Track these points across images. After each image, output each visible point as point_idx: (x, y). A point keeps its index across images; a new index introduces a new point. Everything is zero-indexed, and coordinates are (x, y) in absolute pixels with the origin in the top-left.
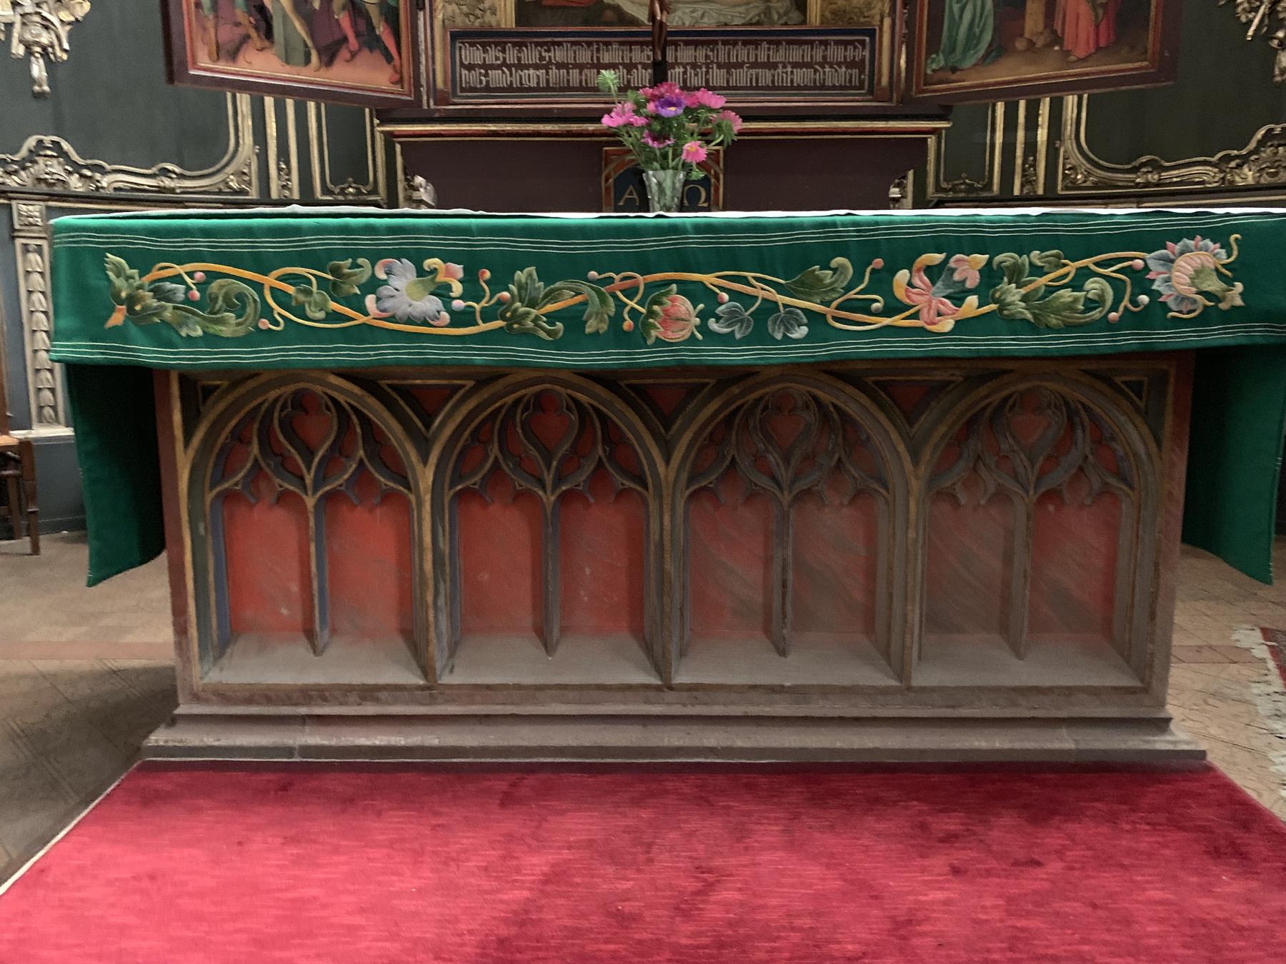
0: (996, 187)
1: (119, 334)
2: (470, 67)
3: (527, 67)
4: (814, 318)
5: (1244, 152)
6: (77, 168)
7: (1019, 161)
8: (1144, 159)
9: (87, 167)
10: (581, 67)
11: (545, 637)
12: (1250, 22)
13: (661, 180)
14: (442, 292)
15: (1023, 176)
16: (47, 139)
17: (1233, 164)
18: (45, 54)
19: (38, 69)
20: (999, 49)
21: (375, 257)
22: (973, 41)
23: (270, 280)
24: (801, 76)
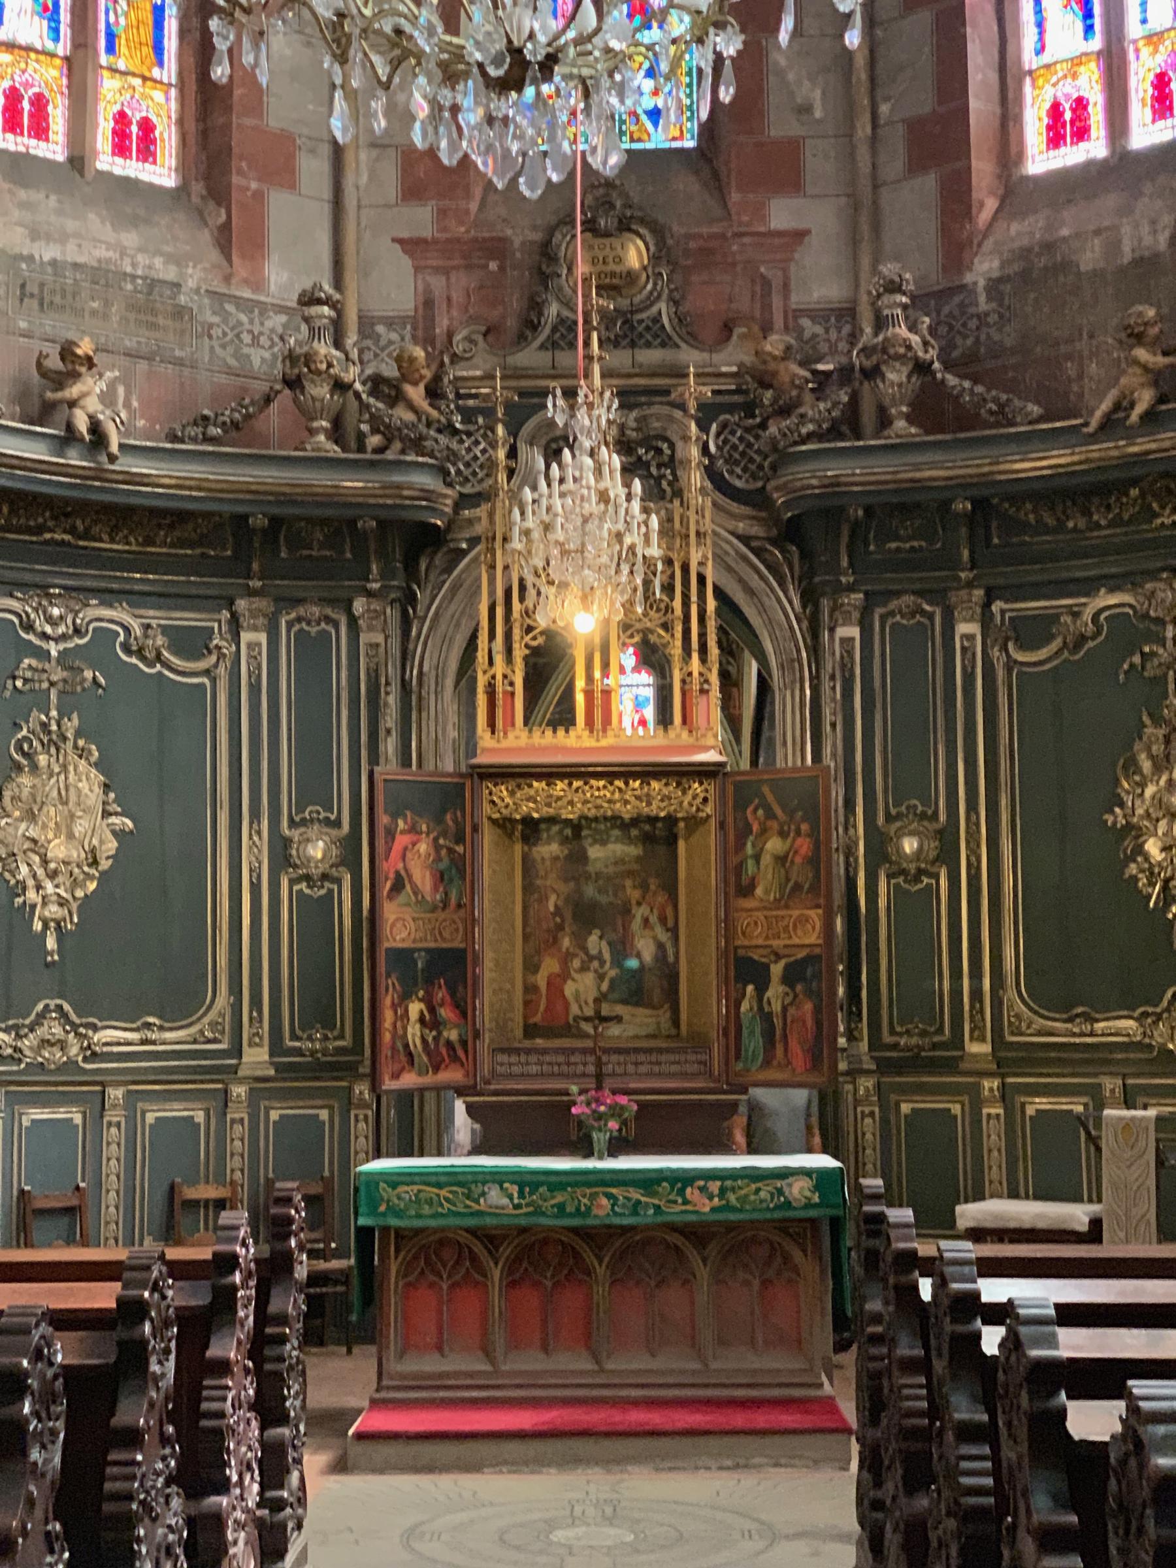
0: (947, 1031)
2: (502, 1064)
4: (657, 1208)
5: (1158, 1010)
6: (75, 1027)
7: (967, 1007)
8: (1080, 1010)
9: (81, 1025)
10: (559, 1065)
11: (545, 1348)
12: (1150, 896)
13: (600, 1139)
14: (511, 1197)
15: (972, 1021)
16: (52, 1003)
17: (1149, 1020)
18: (58, 927)
19: (51, 943)
20: (767, 1063)
21: (484, 1184)
24: (674, 1068)
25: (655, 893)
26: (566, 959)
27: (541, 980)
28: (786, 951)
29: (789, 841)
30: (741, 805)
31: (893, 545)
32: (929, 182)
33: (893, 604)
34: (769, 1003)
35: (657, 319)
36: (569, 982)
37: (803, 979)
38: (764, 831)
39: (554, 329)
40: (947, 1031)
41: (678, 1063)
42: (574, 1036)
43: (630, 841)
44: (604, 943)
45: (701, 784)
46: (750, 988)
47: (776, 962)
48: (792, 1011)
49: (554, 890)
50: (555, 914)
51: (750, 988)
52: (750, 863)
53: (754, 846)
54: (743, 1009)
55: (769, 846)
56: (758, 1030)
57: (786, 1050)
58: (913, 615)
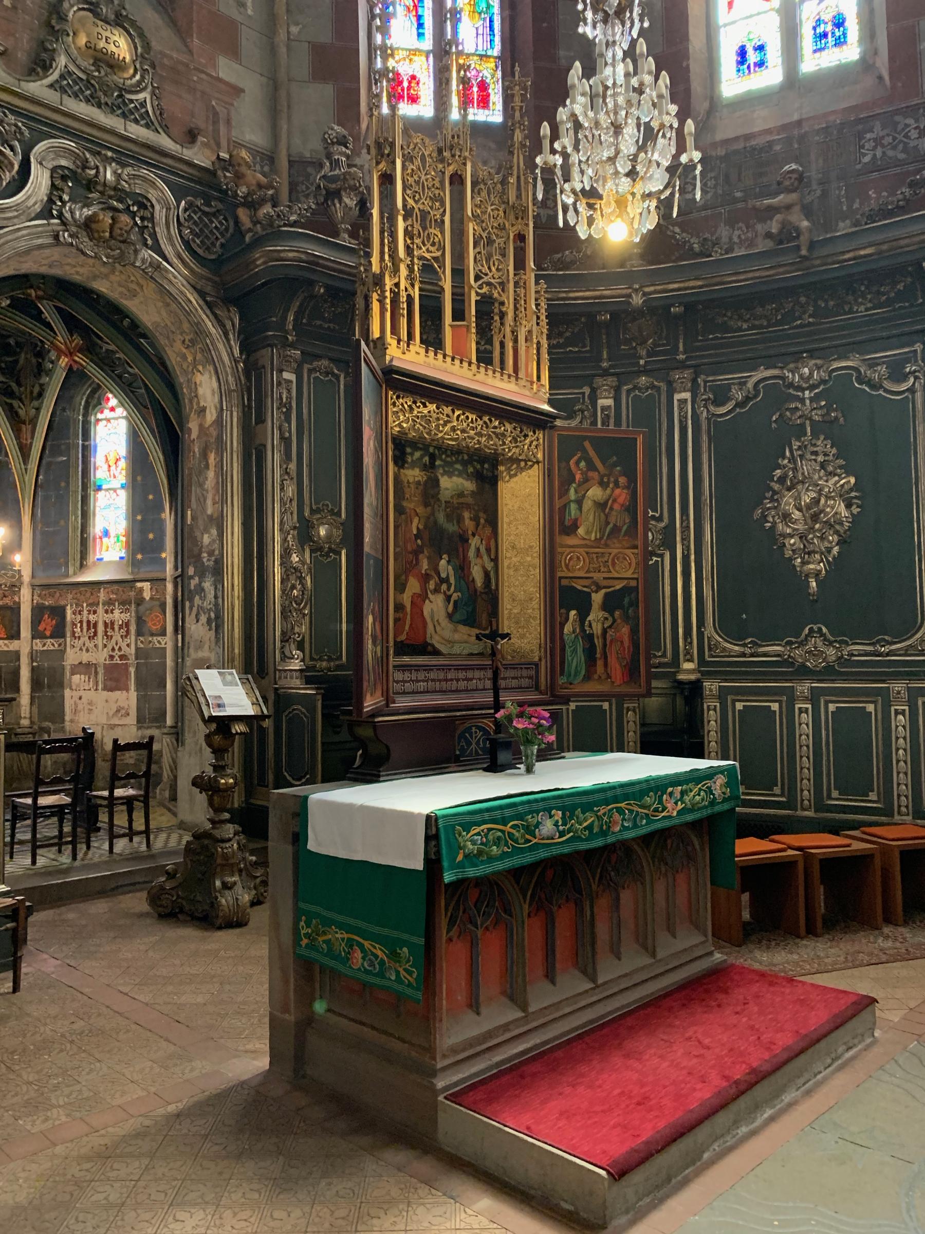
0: (344, 658)
1: (461, 865)
2: (397, 682)
3: (420, 681)
10: (440, 681)
20: (588, 677)
22: (577, 673)
23: (508, 828)
25: (484, 527)
26: (426, 578)
27: (406, 598)
28: (605, 583)
29: (608, 491)
30: (564, 457)
31: (318, 323)
32: (327, 91)
33: (315, 364)
34: (590, 626)
35: (143, 104)
36: (427, 601)
37: (620, 607)
38: (586, 480)
39: (62, 77)
40: (344, 658)
41: (516, 678)
42: (430, 654)
43: (469, 477)
44: (450, 567)
45: (535, 433)
46: (573, 613)
47: (596, 592)
48: (610, 633)
49: (417, 515)
50: (417, 537)
51: (573, 613)
52: (573, 506)
53: (576, 491)
54: (566, 631)
55: (590, 493)
56: (580, 650)
57: (606, 665)
58: (327, 374)
